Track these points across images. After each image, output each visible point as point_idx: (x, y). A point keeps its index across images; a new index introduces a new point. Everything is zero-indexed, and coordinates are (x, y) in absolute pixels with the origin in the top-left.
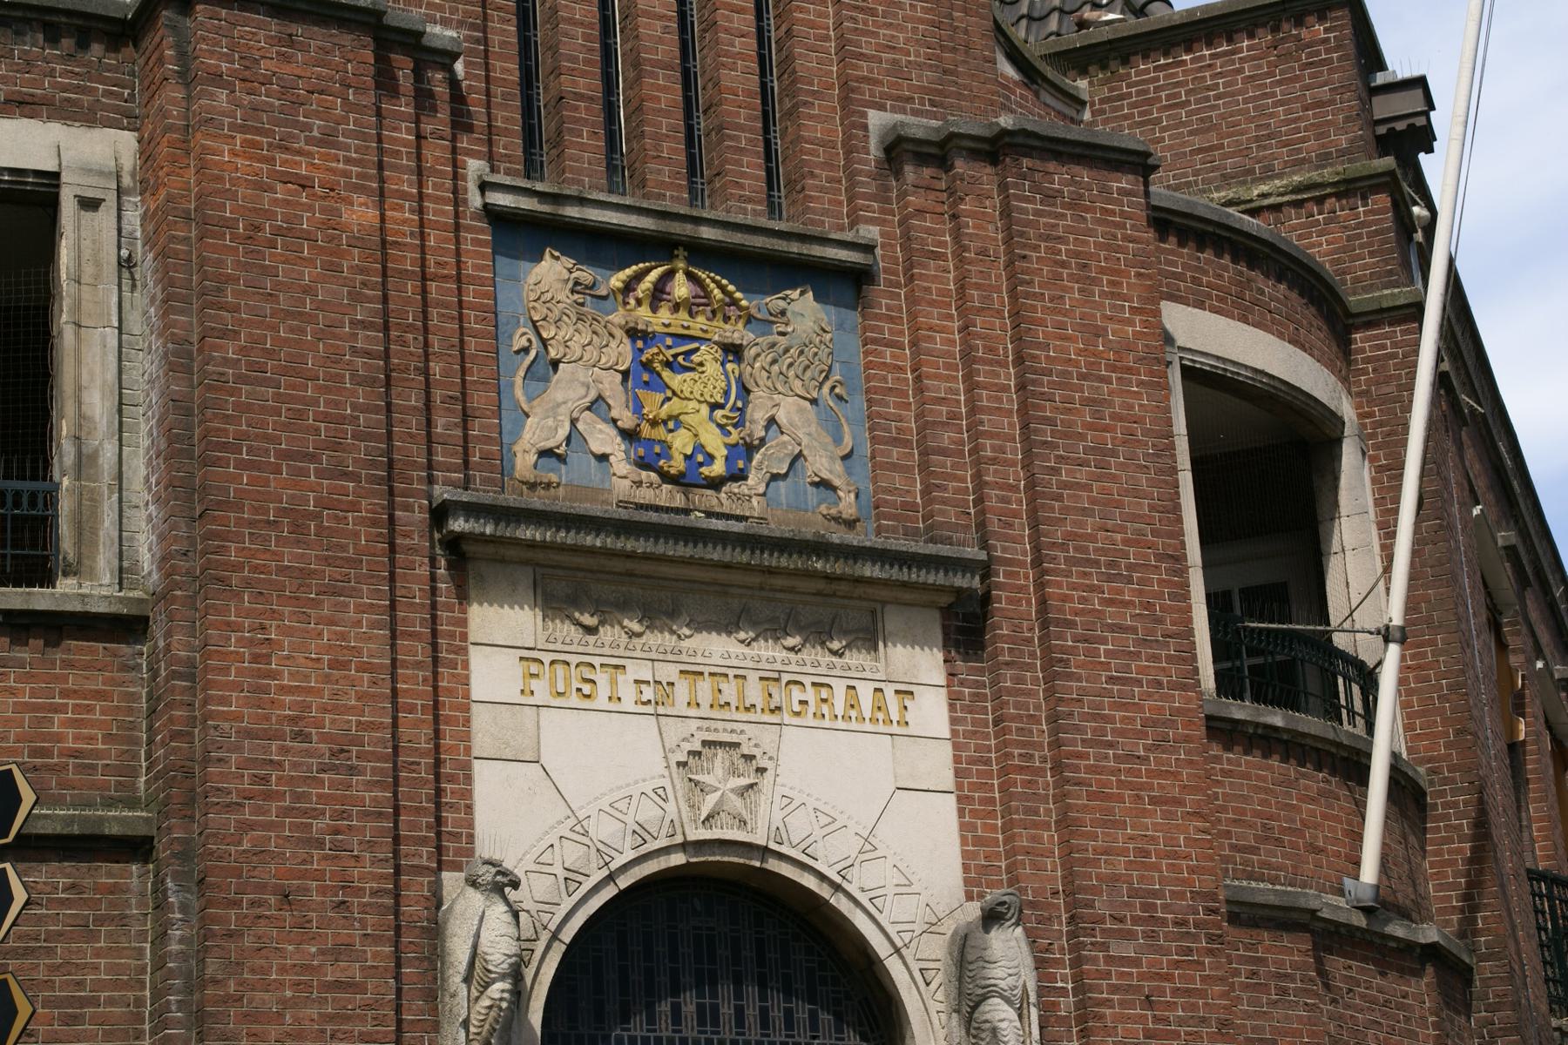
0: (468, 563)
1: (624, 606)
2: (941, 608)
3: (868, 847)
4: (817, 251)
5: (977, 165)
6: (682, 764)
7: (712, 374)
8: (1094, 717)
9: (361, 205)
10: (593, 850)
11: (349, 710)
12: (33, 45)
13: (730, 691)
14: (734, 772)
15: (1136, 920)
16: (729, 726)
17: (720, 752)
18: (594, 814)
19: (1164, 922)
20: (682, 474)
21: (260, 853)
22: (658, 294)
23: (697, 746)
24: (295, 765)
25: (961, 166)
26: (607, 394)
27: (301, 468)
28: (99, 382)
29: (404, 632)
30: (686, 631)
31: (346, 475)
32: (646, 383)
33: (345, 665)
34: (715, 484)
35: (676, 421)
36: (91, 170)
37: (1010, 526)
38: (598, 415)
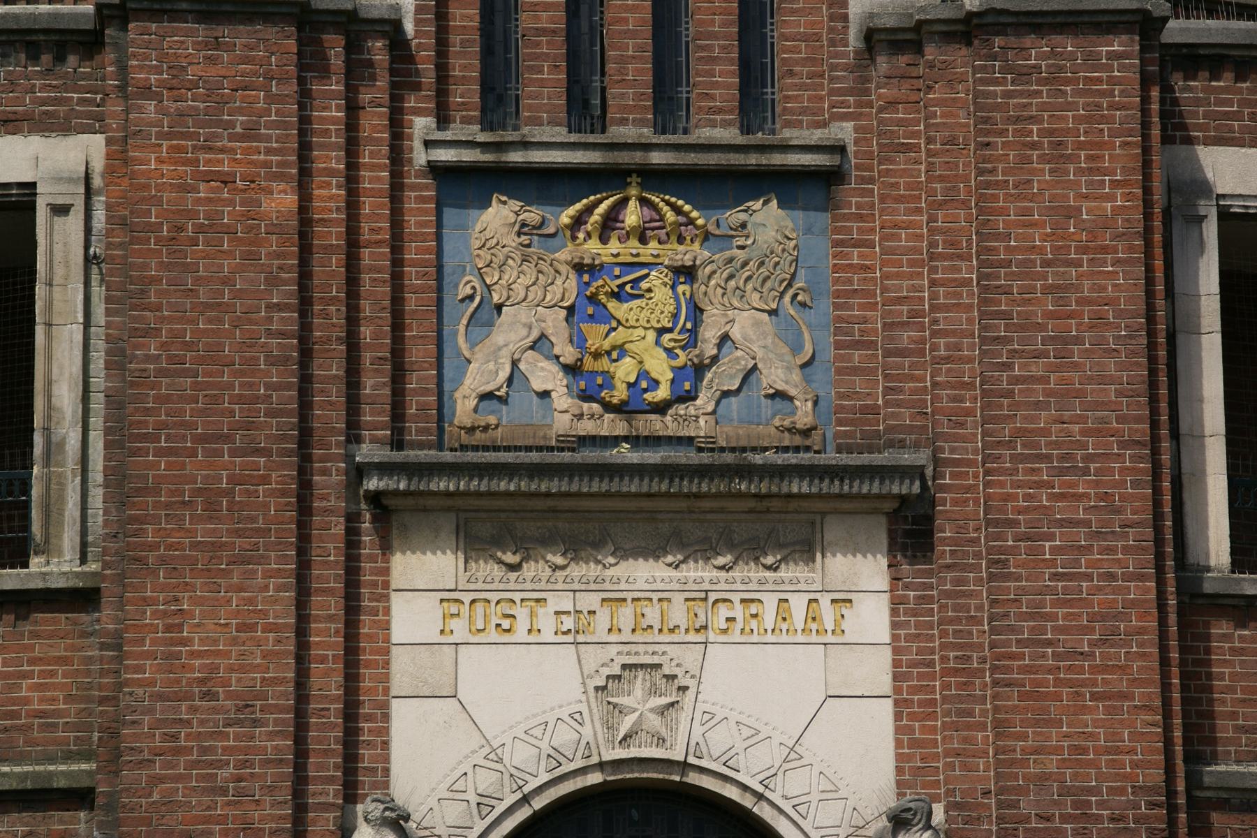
0: (389, 517)
1: (547, 541)
2: (887, 514)
3: (793, 753)
4: (778, 159)
5: (950, 48)
6: (605, 688)
7: (661, 295)
8: (1031, 616)
9: (280, 192)
10: (506, 776)
11: (255, 668)
12: (17, 65)
13: (652, 614)
14: (654, 691)
15: (1065, 818)
16: (650, 648)
17: (640, 674)
18: (509, 742)
19: (1098, 819)
20: (624, 403)
21: (169, 803)
22: (610, 224)
23: (616, 670)
24: (202, 722)
25: (931, 52)
26: (549, 332)
27: (216, 449)
28: (67, 375)
29: (317, 590)
30: (611, 560)
31: (258, 452)
32: (591, 316)
33: (251, 628)
34: (661, 408)
35: (621, 350)
36: (61, 179)
37: (962, 425)
38: (542, 354)
